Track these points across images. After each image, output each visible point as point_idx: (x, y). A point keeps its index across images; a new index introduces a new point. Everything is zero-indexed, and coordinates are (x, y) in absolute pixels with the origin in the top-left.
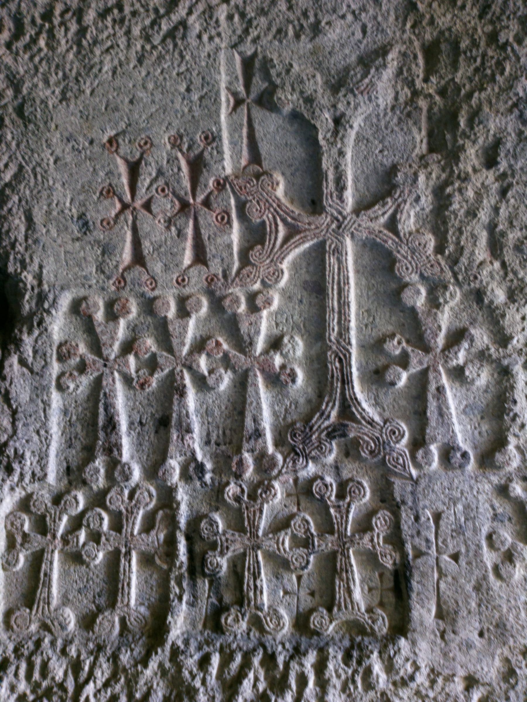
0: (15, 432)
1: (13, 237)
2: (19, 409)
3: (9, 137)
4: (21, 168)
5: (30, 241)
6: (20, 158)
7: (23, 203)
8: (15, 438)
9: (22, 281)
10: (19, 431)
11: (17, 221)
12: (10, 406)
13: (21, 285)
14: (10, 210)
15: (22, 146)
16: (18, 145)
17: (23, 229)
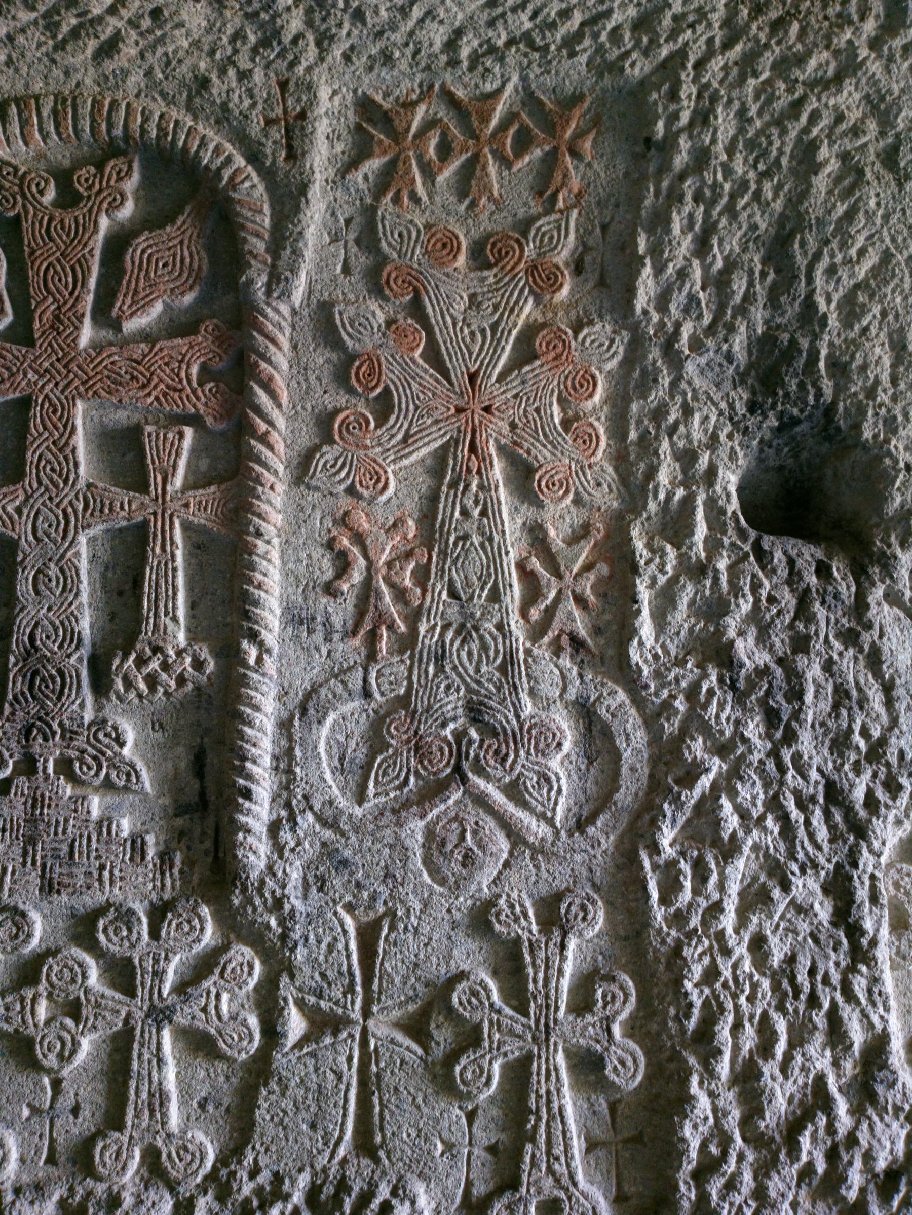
0: (894, 722)
1: (872, 377)
2: (898, 682)
3: (872, 203)
4: (887, 257)
5: (902, 386)
6: (888, 240)
7: (891, 317)
8: (897, 731)
9: (889, 454)
10: (901, 720)
11: (877, 350)
12: (878, 674)
13: (887, 461)
14: (866, 330)
15: (894, 220)
16: (886, 217)
17: (887, 362)
